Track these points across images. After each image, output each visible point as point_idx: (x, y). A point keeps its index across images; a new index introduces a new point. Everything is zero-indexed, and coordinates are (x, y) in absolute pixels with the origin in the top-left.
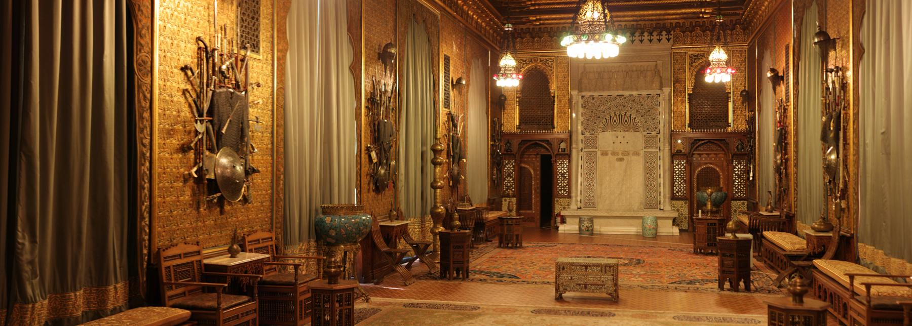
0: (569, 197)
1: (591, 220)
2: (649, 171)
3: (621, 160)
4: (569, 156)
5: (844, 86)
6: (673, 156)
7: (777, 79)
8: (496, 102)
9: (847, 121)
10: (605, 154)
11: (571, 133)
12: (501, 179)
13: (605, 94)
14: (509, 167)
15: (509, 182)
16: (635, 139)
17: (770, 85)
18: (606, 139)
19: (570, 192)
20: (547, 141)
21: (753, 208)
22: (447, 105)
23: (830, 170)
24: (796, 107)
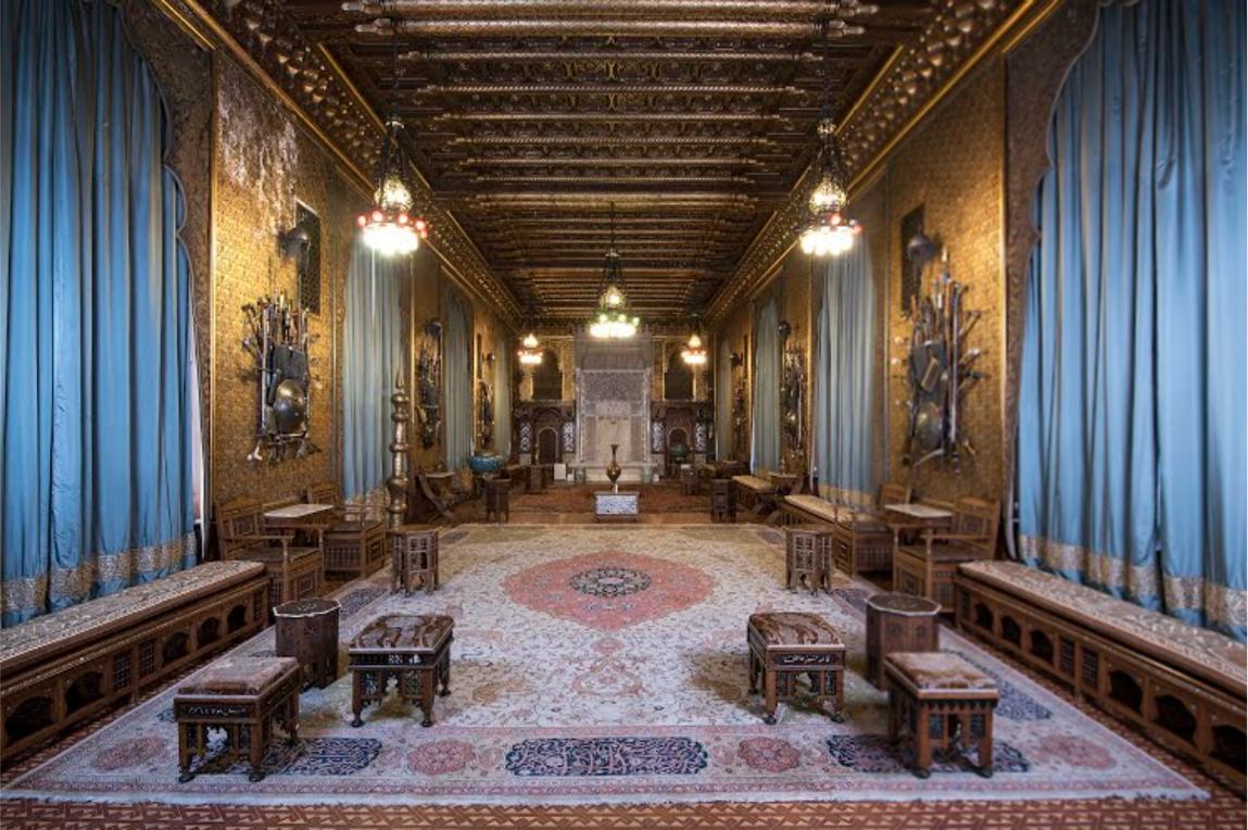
0: (574, 452)
1: (584, 470)
2: (636, 432)
3: (614, 423)
4: (574, 420)
5: (802, 361)
6: (653, 421)
7: (737, 361)
8: (516, 375)
9: (805, 391)
10: (601, 418)
11: (575, 402)
12: (519, 439)
13: (601, 371)
14: (526, 429)
15: (525, 440)
16: (620, 408)
17: (729, 365)
18: (603, 407)
19: (574, 448)
20: (556, 409)
21: (711, 458)
22: (479, 376)
23: (790, 429)
24: (753, 382)
